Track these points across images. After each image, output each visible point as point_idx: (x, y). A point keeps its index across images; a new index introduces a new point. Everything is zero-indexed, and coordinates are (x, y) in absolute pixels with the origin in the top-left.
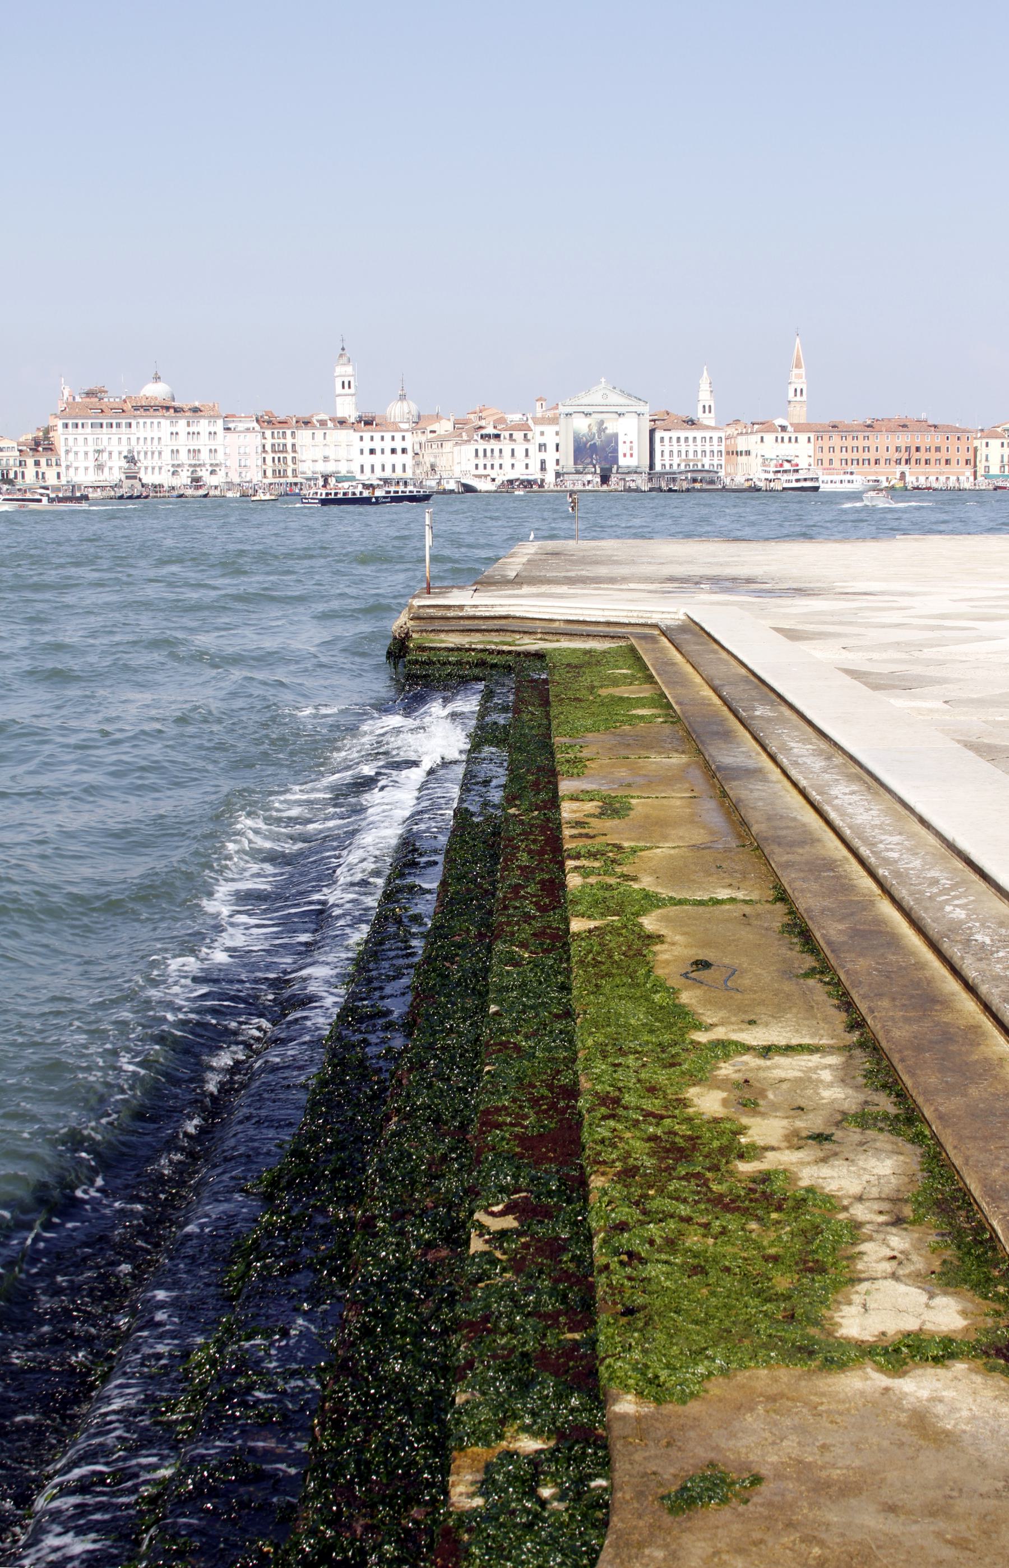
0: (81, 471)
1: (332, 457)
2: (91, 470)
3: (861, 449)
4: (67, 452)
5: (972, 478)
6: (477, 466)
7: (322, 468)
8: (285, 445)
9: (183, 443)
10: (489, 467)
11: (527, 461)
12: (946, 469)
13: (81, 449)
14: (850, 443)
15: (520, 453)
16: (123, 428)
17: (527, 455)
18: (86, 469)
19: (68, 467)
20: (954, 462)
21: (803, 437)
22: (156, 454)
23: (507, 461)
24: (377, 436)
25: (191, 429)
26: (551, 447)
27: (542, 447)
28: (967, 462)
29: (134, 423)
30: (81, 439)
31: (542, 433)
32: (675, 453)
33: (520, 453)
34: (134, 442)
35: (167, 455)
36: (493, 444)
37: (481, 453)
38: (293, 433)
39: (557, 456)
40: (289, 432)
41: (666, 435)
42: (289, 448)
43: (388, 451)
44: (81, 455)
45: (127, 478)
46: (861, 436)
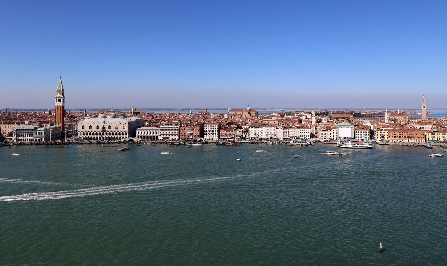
0: (252, 135)
1: (295, 134)
2: (254, 135)
3: (399, 134)
4: (250, 132)
5: (425, 141)
6: (321, 136)
7: (293, 135)
8: (287, 131)
9: (269, 131)
10: (323, 136)
11: (331, 135)
12: (419, 139)
13: (252, 132)
14: (396, 133)
15: (329, 134)
16: (259, 128)
17: (330, 134)
18: (253, 135)
19: (250, 135)
20: (420, 137)
21: (386, 132)
22: (265, 133)
23: (327, 135)
24: (304, 130)
25: (271, 129)
26: (335, 133)
27: (333, 133)
28: (424, 137)
29: (261, 127)
30: (252, 130)
31: (333, 130)
32: (359, 135)
33: (329, 134)
34: (261, 131)
35: (266, 133)
36: (325, 132)
37: (322, 134)
38: (288, 129)
39: (336, 134)
40: (288, 129)
41: (358, 131)
42: (288, 132)
43: (304, 133)
44: (252, 133)
45: (257, 138)
46: (399, 132)
